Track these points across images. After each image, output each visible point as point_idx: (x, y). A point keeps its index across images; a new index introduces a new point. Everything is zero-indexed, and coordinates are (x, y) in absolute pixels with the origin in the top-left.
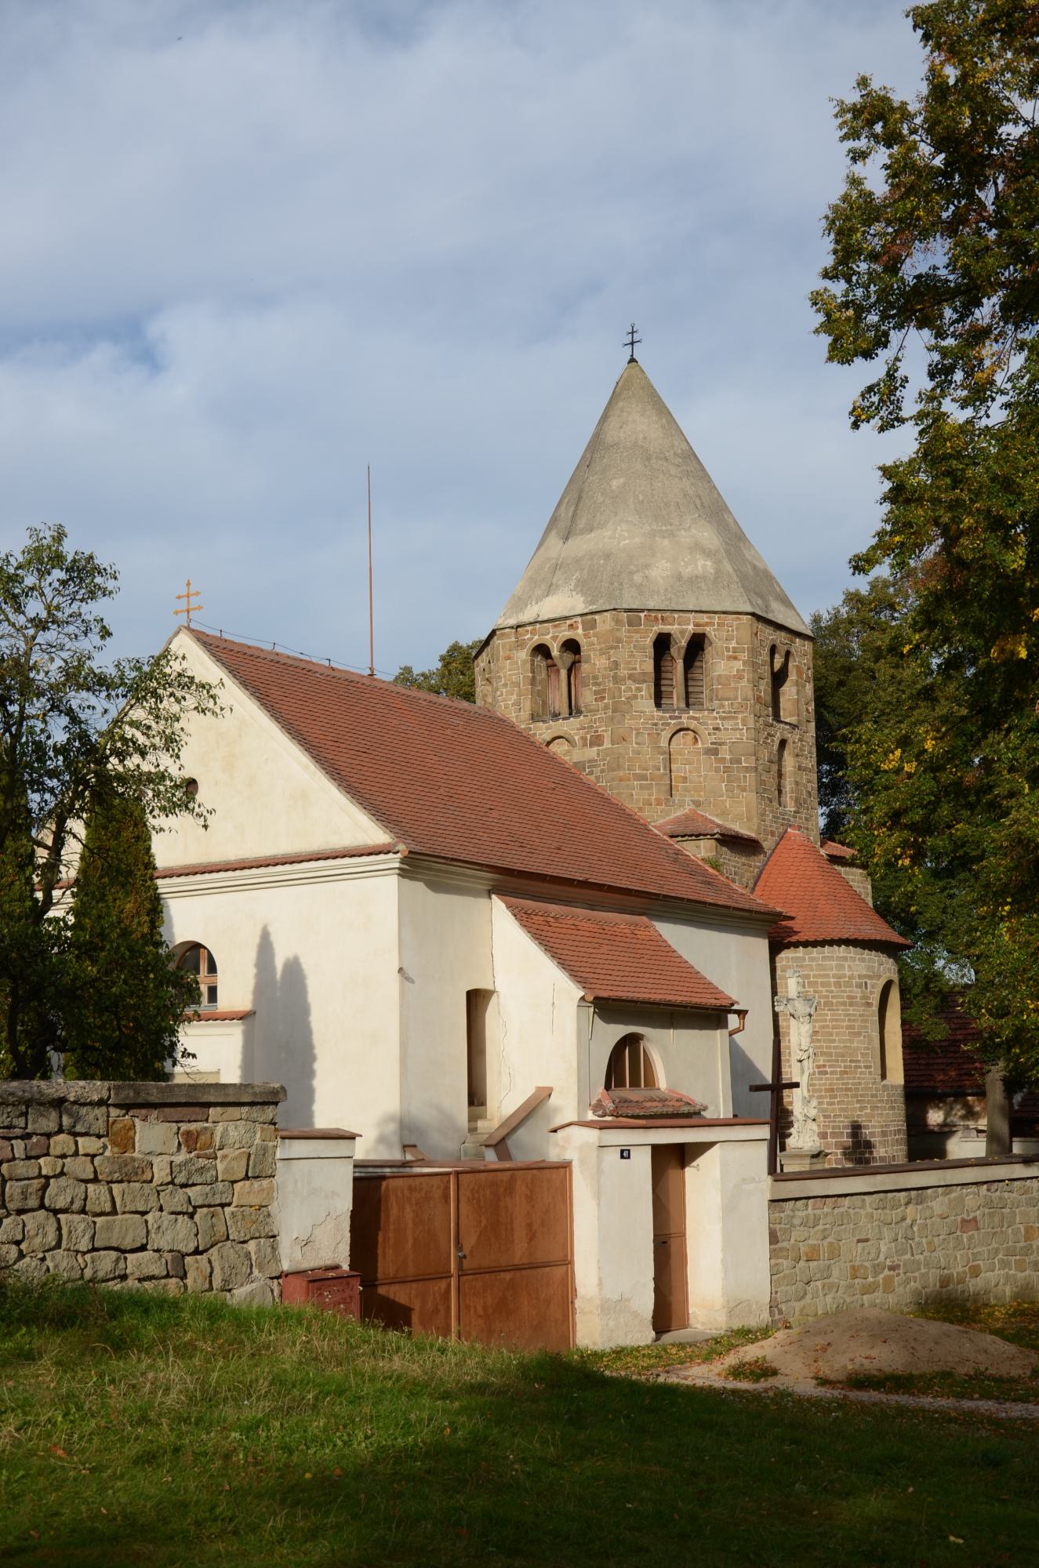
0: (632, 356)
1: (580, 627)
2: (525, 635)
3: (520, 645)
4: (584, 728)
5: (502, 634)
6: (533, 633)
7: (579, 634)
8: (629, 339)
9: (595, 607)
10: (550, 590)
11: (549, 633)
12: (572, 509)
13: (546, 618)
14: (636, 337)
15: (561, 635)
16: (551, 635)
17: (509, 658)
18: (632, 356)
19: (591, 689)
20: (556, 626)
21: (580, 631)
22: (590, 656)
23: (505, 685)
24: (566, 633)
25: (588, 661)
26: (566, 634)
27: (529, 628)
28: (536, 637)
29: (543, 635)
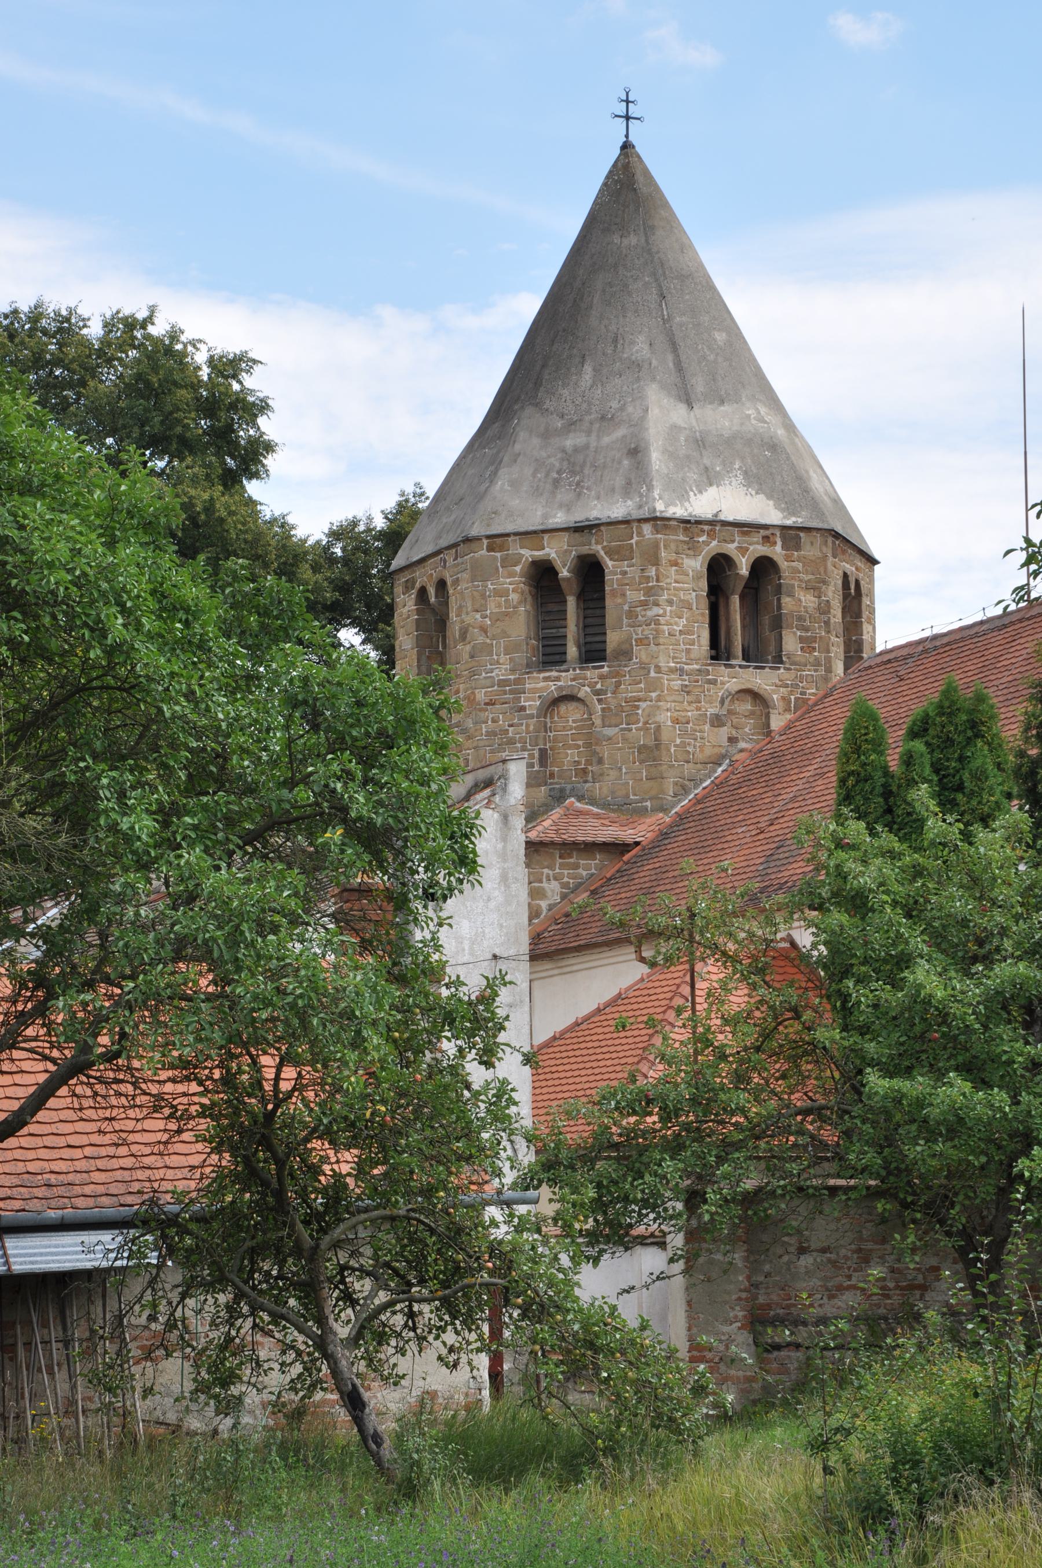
0: (627, 136)
1: (779, 543)
2: (699, 536)
3: (693, 548)
4: (786, 686)
5: (666, 527)
6: (711, 535)
7: (777, 551)
8: (621, 109)
9: (800, 520)
10: (710, 478)
11: (733, 541)
12: (670, 357)
13: (730, 519)
14: (633, 110)
15: (751, 548)
16: (736, 544)
17: (675, 564)
18: (627, 136)
19: (795, 633)
20: (745, 533)
21: (778, 548)
22: (793, 586)
23: (670, 602)
24: (759, 547)
25: (791, 595)
26: (759, 549)
27: (706, 528)
28: (714, 543)
29: (725, 541)
